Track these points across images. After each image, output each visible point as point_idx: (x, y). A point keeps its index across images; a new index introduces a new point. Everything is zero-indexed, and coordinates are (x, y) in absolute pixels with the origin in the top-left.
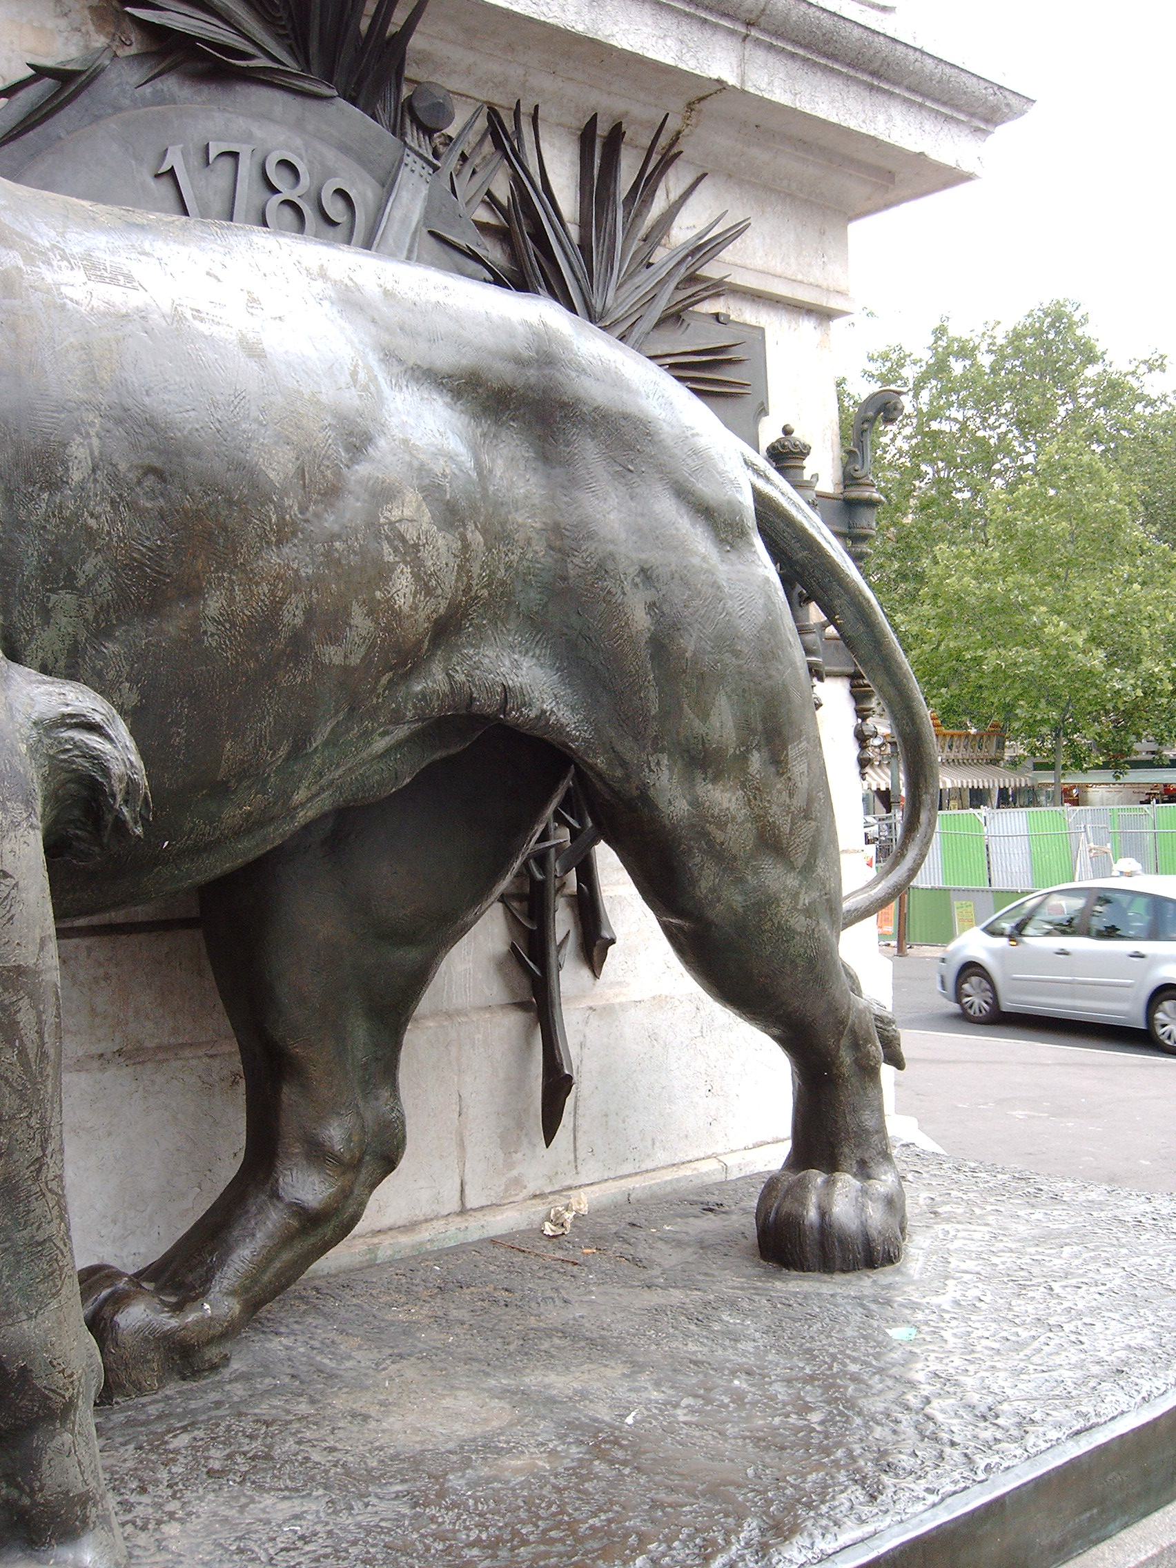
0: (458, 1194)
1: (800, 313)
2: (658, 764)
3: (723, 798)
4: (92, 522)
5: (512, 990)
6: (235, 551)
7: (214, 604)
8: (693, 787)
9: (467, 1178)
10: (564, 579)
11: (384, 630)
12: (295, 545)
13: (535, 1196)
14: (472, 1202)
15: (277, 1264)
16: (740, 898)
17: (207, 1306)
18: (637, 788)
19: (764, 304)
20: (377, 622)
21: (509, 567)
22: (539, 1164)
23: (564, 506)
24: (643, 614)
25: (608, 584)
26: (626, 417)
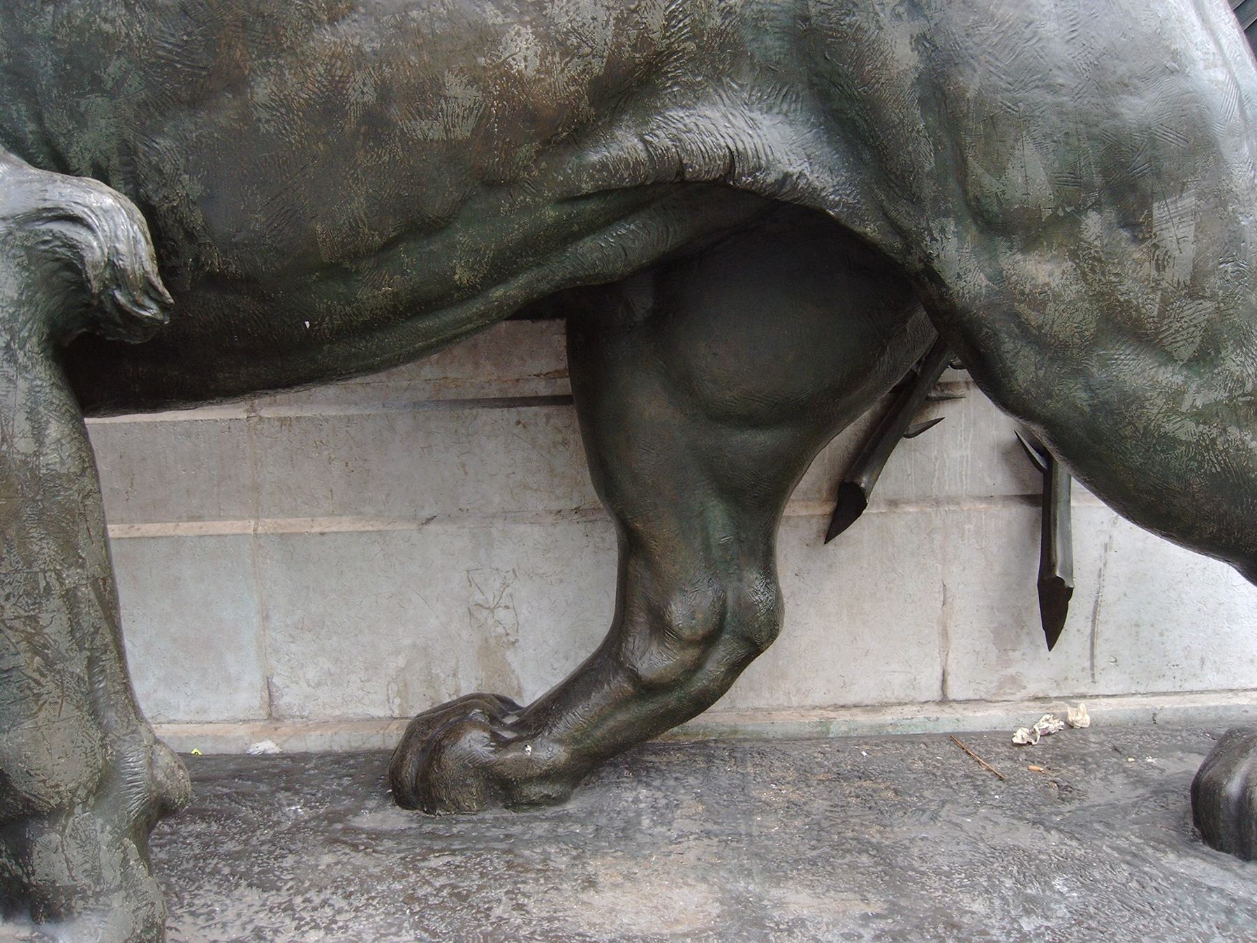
0: (939, 684)
2: (943, 231)
3: (1042, 270)
4: (107, 27)
5: (1022, 482)
6: (276, 35)
7: (263, 90)
8: (993, 257)
9: (952, 668)
10: (806, 19)
11: (500, 97)
12: (355, 21)
13: (1037, 699)
14: (954, 692)
15: (611, 723)
16: (1083, 395)
17: (529, 748)
18: (920, 260)
20: (485, 90)
22: (1040, 668)
24: (908, 50)
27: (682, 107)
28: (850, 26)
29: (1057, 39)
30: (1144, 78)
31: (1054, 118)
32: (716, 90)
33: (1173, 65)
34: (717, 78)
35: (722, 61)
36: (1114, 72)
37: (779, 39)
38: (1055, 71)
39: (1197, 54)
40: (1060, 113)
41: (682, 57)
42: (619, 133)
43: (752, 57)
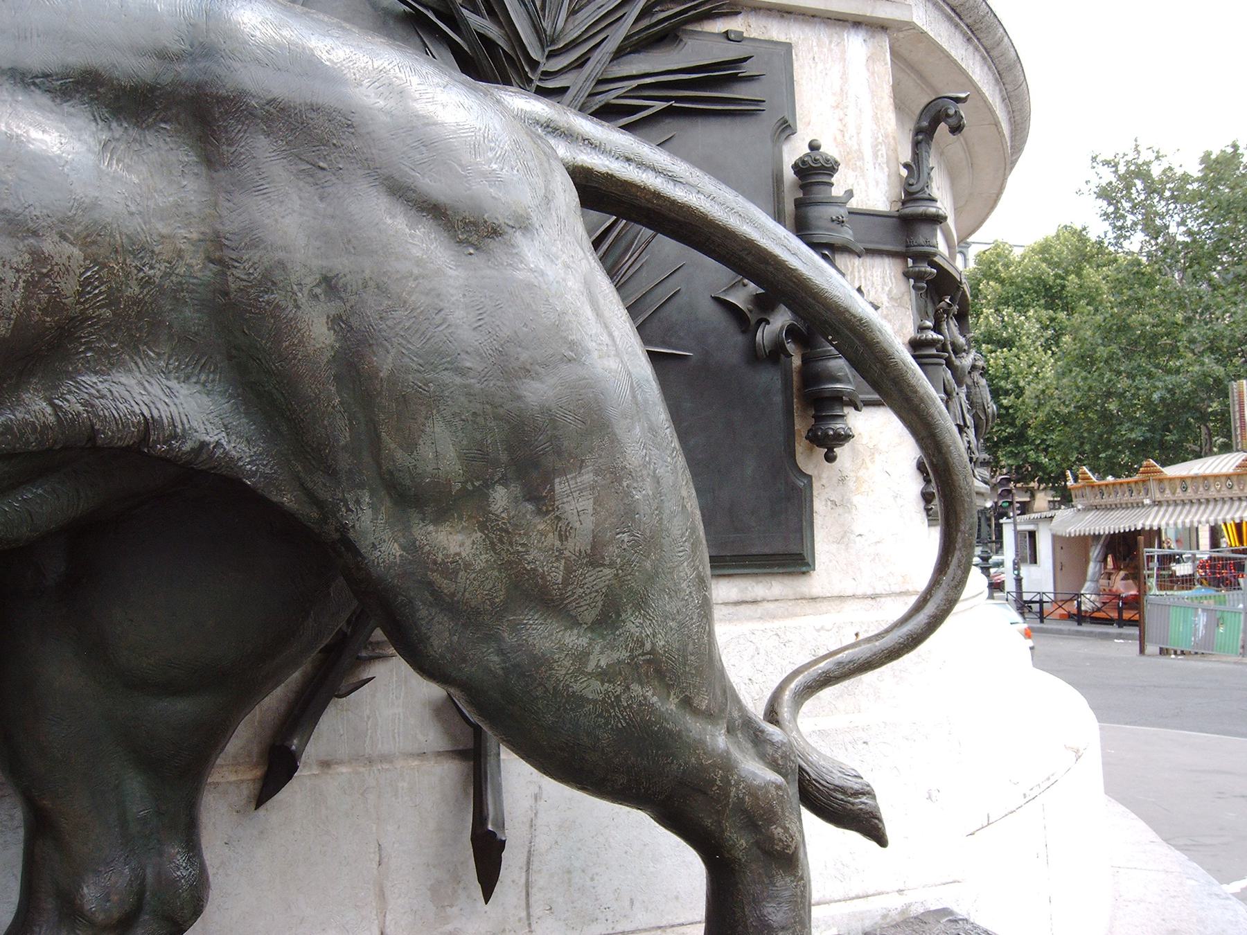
1: (846, 27)
2: (358, 502)
3: (454, 541)
8: (407, 528)
10: (226, 294)
16: (496, 659)
18: (337, 530)
19: (796, 20)
21: (146, 282)
23: (225, 213)
24: (325, 329)
25: (276, 297)
26: (315, 108)
27: (96, 373)
28: (268, 303)
29: (465, 326)
30: (545, 365)
31: (462, 399)
32: (132, 358)
33: (573, 354)
34: (134, 346)
35: (139, 329)
36: (517, 359)
37: (198, 311)
38: (463, 356)
39: (592, 345)
40: (468, 394)
41: (97, 323)
42: (26, 397)
43: (170, 327)
